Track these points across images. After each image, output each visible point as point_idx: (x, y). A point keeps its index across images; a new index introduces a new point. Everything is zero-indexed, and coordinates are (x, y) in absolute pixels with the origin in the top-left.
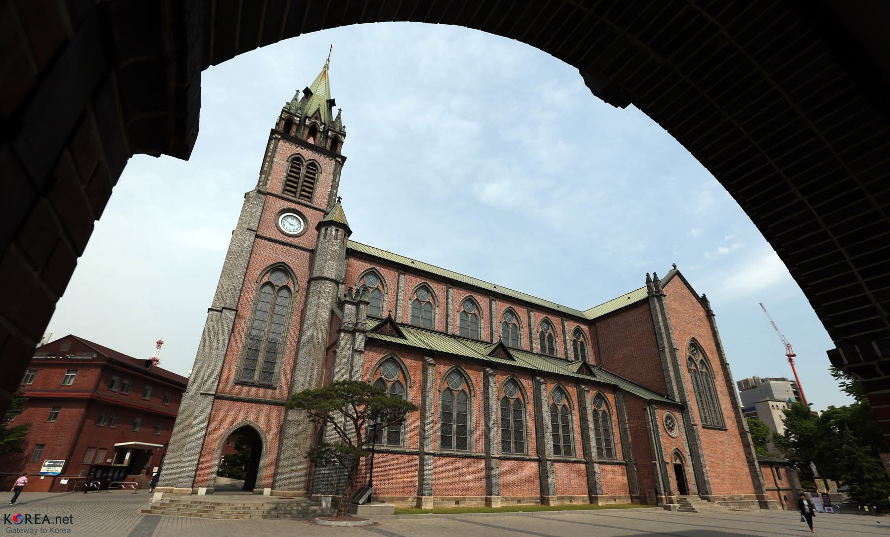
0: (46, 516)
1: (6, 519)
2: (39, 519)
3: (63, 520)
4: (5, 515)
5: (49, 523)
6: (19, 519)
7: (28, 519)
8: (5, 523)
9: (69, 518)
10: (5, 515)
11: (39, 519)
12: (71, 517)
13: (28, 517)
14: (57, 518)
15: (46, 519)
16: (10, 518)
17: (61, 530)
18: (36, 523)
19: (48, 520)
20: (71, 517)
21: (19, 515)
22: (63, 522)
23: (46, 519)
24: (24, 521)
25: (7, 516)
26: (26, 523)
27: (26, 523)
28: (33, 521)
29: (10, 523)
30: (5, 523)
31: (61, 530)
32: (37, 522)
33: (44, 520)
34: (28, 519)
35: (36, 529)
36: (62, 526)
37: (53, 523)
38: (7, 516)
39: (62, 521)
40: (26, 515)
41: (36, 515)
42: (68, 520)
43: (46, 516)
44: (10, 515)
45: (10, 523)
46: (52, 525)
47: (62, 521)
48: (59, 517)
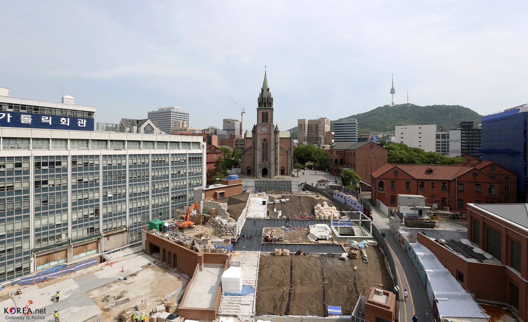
0: (30, 308)
1: (5, 311)
2: (25, 310)
3: (40, 311)
4: (5, 308)
5: (32, 313)
6: (13, 311)
7: (19, 311)
8: (5, 313)
9: (44, 311)
10: (5, 308)
11: (25, 310)
12: (45, 310)
13: (19, 309)
14: (36, 310)
15: (30, 311)
16: (8, 311)
17: (39, 318)
18: (23, 313)
19: (31, 311)
20: (45, 310)
21: (13, 308)
22: (40, 313)
23: (30, 311)
24: (16, 312)
25: (6, 309)
26: (18, 313)
27: (18, 313)
28: (22, 313)
29: (8, 313)
30: (5, 313)
31: (39, 318)
32: (24, 313)
33: (29, 311)
34: (19, 311)
35: (24, 317)
36: (40, 315)
37: (34, 313)
38: (6, 309)
39: (39, 313)
40: (18, 309)
41: (23, 308)
42: (43, 311)
43: (30, 308)
44: (7, 308)
45: (8, 313)
46: (33, 315)
47: (39, 313)
48: (38, 309)
